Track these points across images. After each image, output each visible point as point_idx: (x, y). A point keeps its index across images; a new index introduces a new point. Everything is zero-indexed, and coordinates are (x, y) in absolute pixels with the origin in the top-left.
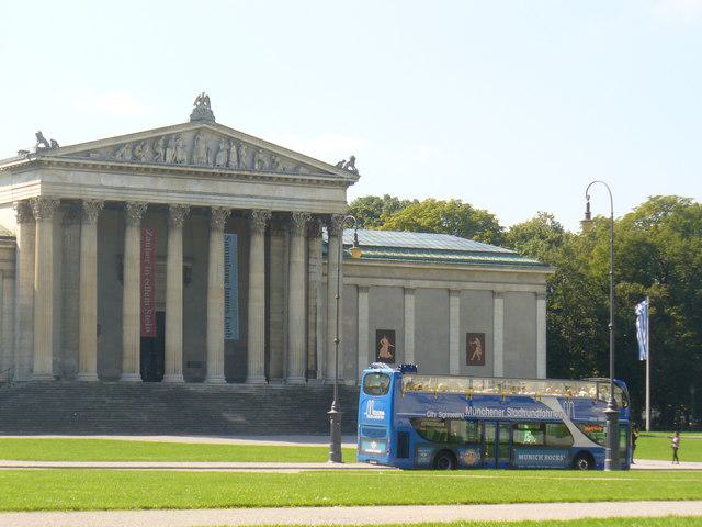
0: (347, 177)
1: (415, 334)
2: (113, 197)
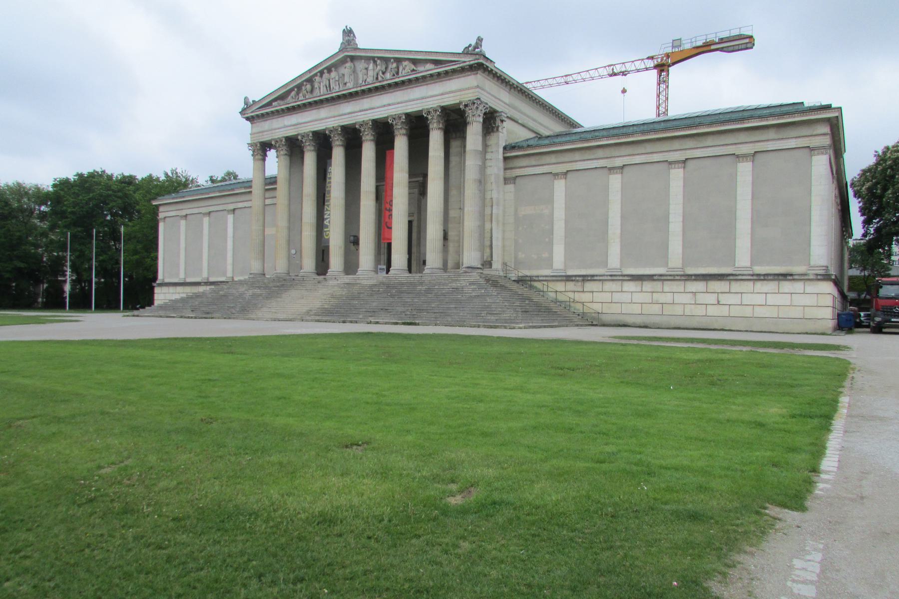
0: (469, 60)
1: (622, 217)
2: (291, 133)
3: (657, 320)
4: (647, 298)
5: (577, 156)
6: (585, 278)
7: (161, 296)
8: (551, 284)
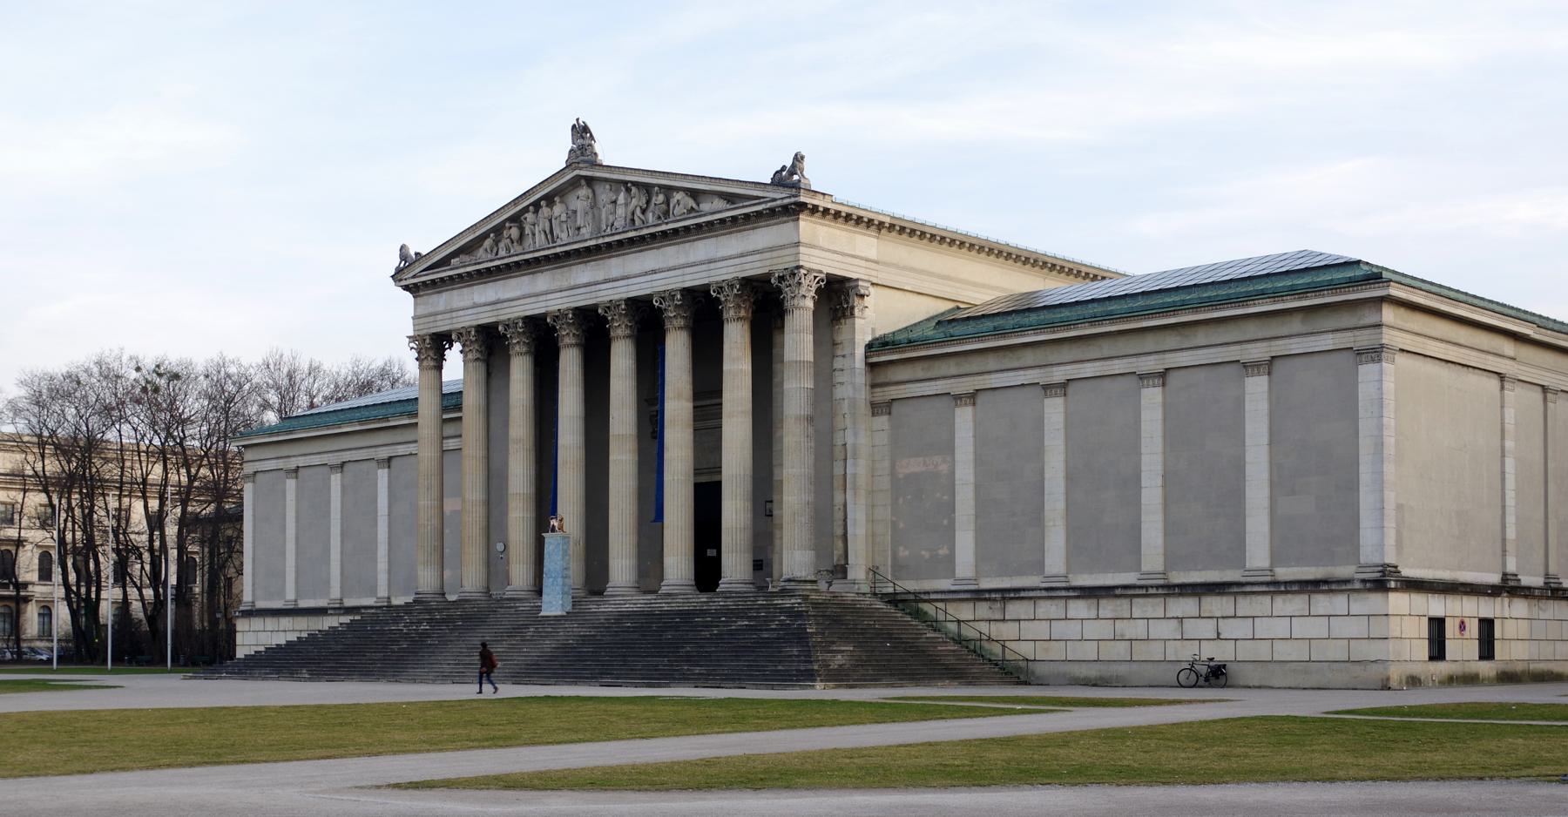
0: (781, 197)
2: (486, 318)
3: (1122, 669)
4: (1102, 629)
5: (991, 362)
6: (1008, 595)
7: (251, 638)
8: (951, 608)
